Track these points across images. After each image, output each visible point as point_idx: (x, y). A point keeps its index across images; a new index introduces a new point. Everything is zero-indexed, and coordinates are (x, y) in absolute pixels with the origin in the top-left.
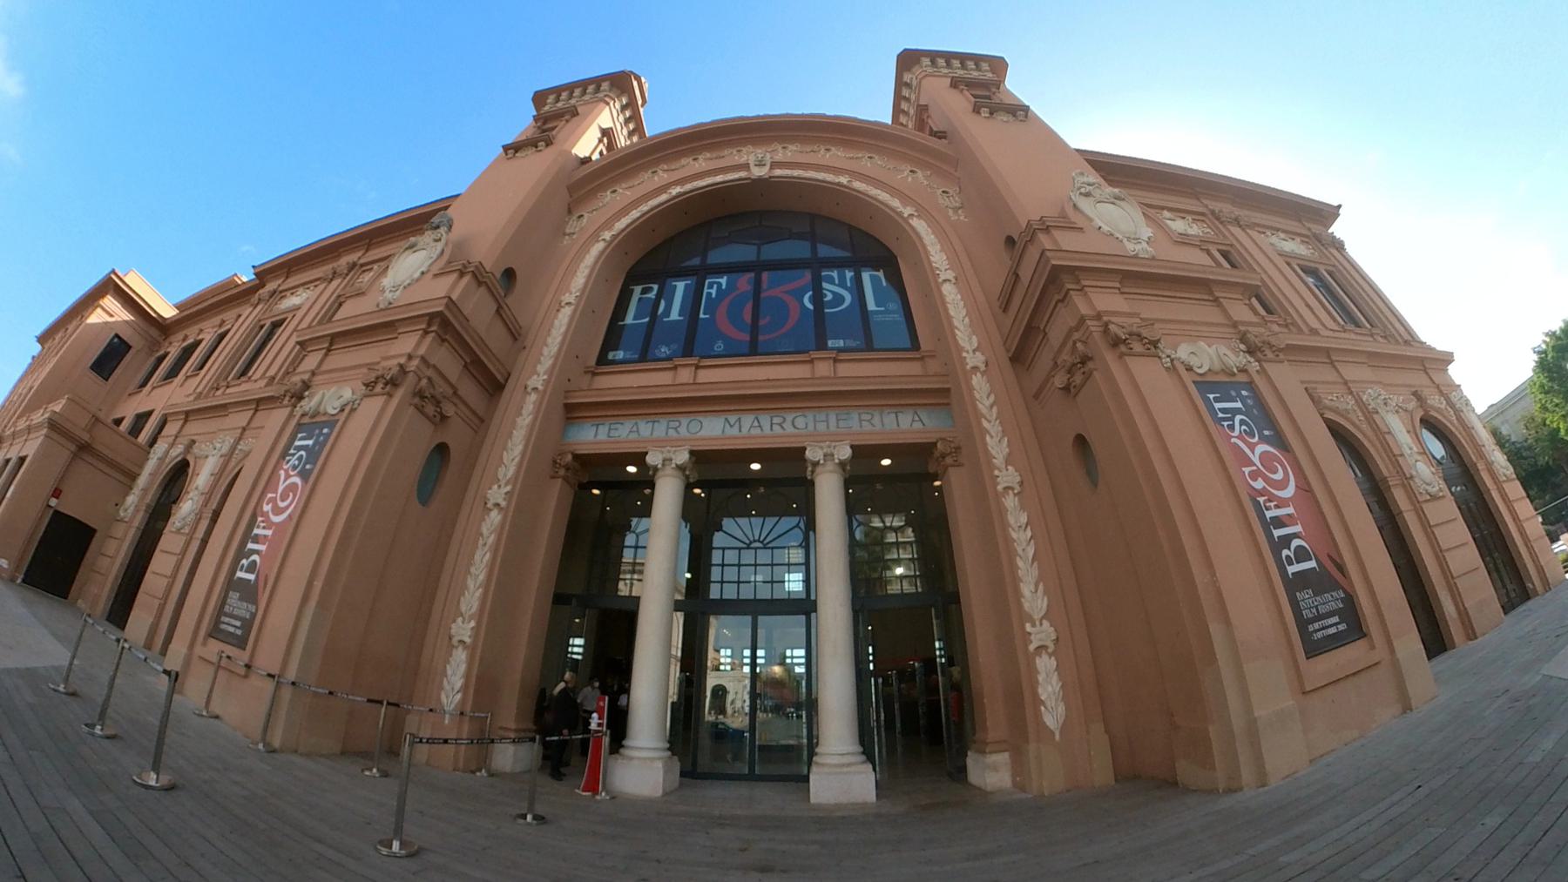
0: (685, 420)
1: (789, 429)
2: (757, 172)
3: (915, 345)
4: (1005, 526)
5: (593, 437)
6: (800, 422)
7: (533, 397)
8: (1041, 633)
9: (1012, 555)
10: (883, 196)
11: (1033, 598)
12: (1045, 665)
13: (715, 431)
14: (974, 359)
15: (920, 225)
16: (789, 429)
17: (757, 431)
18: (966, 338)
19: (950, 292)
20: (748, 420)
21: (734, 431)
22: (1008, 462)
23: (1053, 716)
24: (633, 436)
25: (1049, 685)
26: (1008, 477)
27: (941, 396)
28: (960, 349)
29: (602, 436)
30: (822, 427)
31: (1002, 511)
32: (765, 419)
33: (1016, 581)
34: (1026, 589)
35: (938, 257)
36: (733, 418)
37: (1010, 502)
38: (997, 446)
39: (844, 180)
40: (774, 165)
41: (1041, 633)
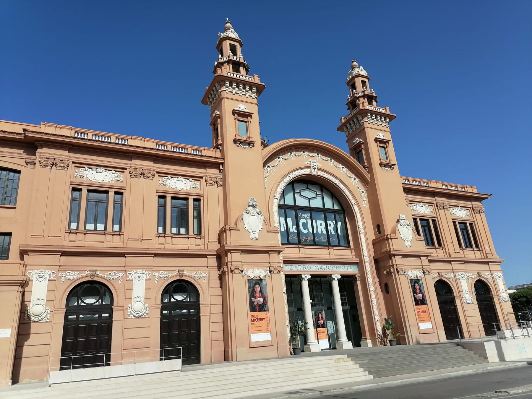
14: (367, 259)
17: (321, 270)
21: (317, 270)
24: (296, 270)
29: (289, 269)
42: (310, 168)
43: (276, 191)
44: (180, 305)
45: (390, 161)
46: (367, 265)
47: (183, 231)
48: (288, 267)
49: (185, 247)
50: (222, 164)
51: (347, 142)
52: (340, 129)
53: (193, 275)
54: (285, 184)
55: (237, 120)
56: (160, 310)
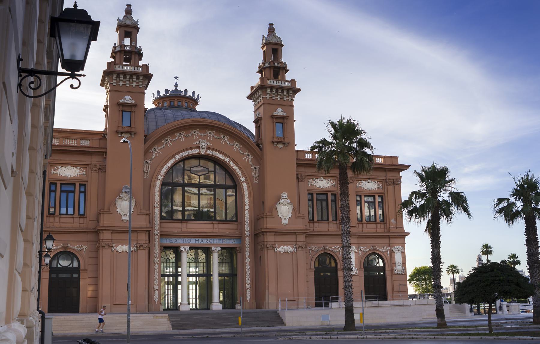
0: (187, 239)
1: (209, 243)
2: (203, 152)
3: (236, 221)
4: (246, 268)
5: (167, 242)
6: (211, 241)
7: (157, 237)
8: (248, 286)
9: (246, 273)
10: (237, 170)
11: (248, 281)
12: (248, 291)
13: (193, 242)
14: (247, 234)
15: (245, 185)
16: (209, 243)
18: (247, 228)
19: (247, 212)
20: (200, 240)
21: (197, 242)
22: (249, 257)
23: (248, 299)
25: (248, 294)
26: (248, 260)
27: (240, 237)
28: (245, 231)
29: (168, 242)
30: (215, 242)
31: (246, 266)
32: (204, 240)
33: (246, 278)
34: (247, 279)
35: (247, 201)
36: (197, 239)
37: (247, 264)
38: (247, 254)
39: (227, 160)
40: (208, 148)
41: (248, 286)
42: (198, 148)
43: (159, 173)
44: (65, 269)
45: (284, 139)
46: (247, 239)
47: (70, 211)
48: (168, 240)
49: (70, 225)
50: (106, 152)
51: (254, 112)
52: (249, 97)
53: (75, 247)
54: (169, 165)
55: (121, 112)
56: (48, 273)
